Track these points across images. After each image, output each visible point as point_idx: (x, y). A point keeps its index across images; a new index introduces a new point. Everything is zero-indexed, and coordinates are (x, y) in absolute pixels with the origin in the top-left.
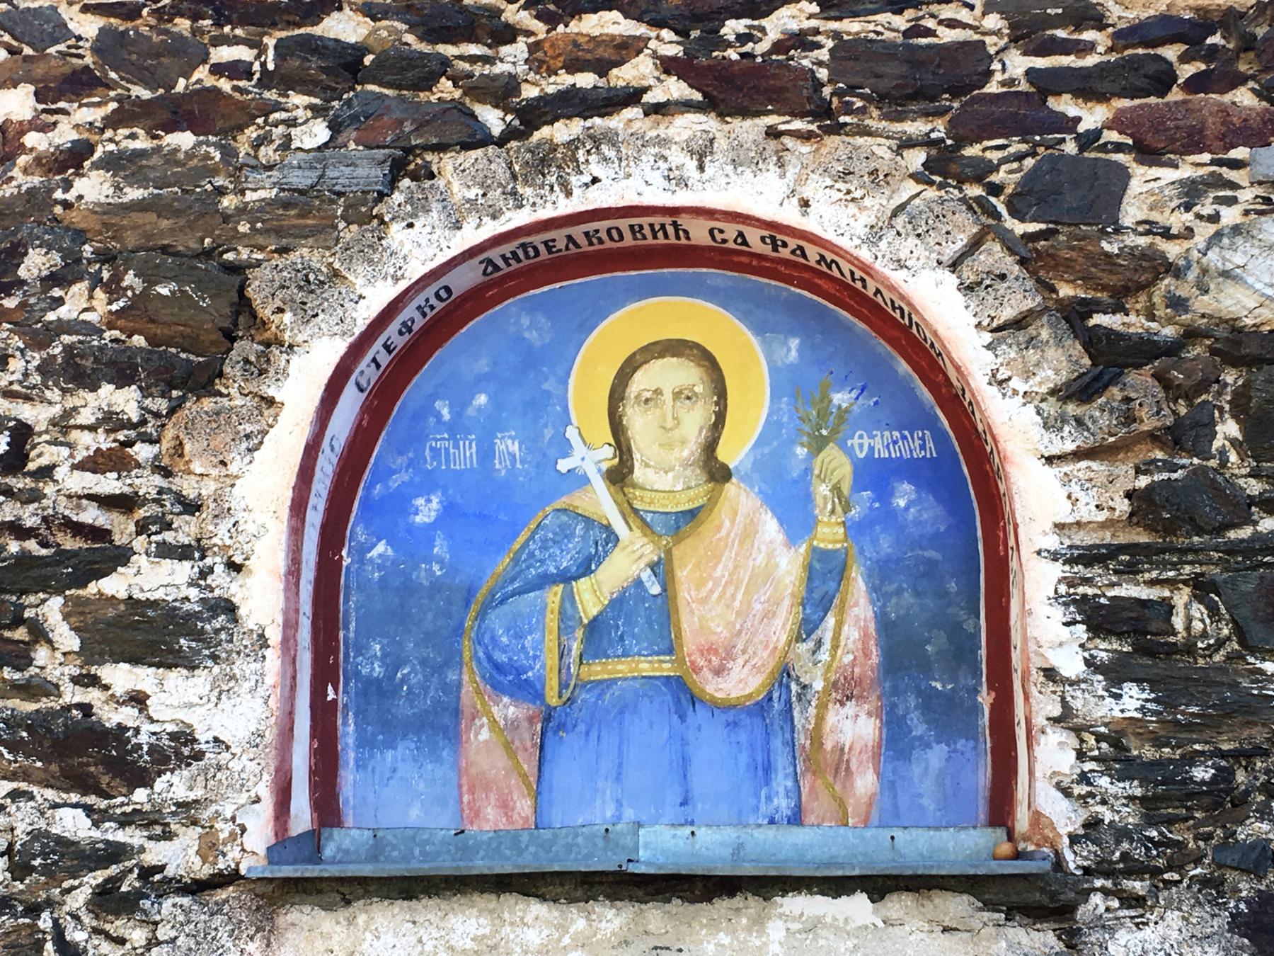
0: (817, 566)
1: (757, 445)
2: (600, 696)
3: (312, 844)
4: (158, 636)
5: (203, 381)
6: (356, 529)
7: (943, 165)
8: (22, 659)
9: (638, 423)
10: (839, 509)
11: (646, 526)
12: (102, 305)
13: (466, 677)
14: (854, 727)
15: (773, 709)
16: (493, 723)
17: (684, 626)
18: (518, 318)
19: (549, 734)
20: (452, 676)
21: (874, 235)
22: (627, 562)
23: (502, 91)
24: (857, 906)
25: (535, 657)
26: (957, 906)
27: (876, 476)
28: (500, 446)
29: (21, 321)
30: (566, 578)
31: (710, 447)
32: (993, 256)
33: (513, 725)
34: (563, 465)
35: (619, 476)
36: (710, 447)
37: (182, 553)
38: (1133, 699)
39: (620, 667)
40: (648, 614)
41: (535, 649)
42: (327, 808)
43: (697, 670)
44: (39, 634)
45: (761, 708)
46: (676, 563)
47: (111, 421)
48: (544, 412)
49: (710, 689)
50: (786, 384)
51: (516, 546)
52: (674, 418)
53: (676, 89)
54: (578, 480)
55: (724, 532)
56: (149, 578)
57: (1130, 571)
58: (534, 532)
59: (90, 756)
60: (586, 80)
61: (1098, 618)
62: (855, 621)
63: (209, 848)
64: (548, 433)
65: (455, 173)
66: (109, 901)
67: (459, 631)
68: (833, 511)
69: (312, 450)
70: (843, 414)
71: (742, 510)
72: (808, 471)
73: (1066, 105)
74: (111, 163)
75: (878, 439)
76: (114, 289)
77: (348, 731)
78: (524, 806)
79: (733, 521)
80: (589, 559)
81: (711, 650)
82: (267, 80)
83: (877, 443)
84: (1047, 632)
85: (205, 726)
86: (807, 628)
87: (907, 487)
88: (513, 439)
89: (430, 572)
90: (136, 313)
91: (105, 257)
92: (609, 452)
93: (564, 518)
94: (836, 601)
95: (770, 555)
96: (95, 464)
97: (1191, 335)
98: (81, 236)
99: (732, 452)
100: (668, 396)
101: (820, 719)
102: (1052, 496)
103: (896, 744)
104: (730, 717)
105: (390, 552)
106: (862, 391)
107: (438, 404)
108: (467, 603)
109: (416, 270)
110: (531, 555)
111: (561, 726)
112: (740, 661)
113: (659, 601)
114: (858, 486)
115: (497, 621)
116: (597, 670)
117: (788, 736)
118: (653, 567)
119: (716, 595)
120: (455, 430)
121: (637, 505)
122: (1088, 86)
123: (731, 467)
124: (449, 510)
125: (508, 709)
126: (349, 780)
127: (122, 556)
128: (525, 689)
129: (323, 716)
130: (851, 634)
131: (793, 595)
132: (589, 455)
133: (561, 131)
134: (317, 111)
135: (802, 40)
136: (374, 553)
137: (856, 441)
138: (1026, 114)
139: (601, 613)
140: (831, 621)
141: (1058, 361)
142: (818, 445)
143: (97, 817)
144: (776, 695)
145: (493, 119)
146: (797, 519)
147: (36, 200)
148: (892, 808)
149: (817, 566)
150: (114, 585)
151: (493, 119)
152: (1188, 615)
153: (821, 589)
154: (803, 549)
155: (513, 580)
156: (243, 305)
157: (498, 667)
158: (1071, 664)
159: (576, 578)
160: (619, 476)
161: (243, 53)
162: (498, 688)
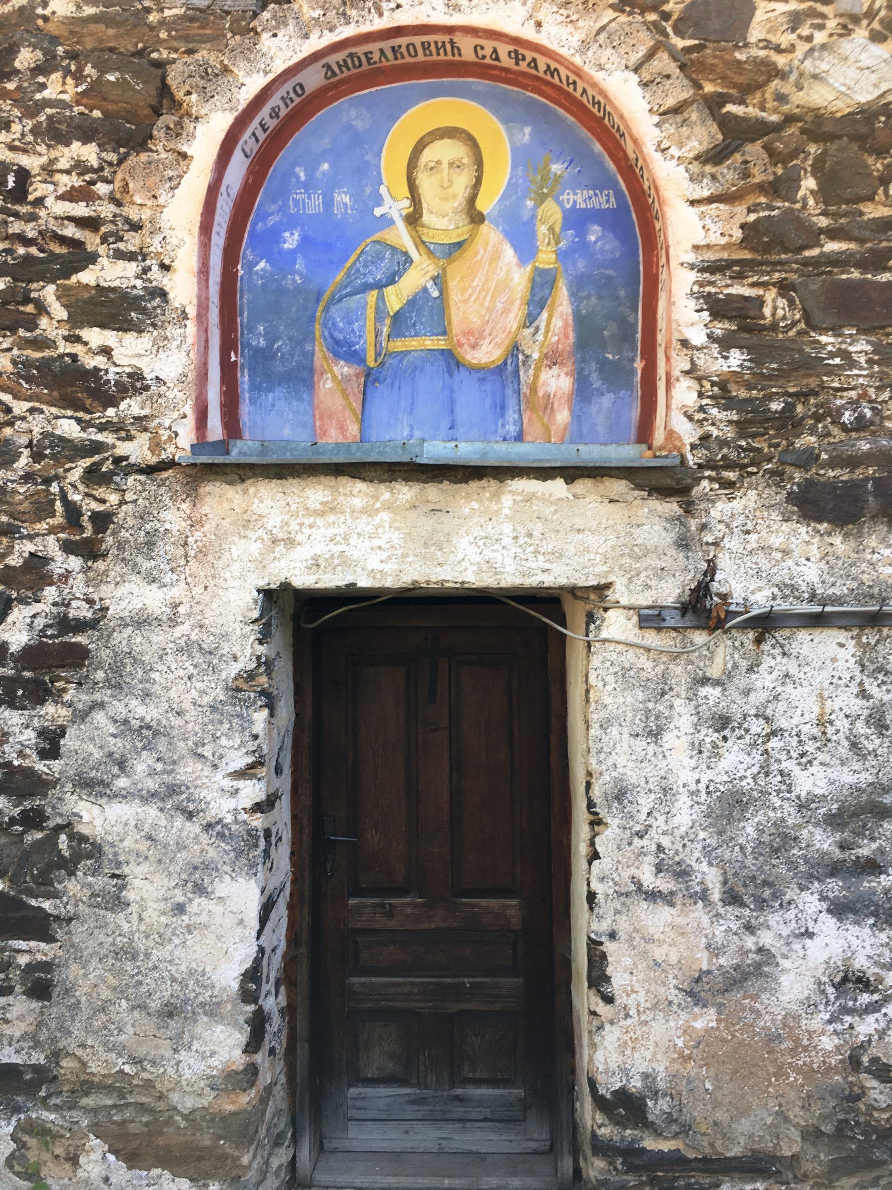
0: (538, 279)
1: (503, 198)
2: (400, 362)
3: (223, 447)
4: (117, 310)
5: (140, 141)
6: (246, 250)
8: (31, 325)
9: (426, 184)
10: (553, 242)
11: (430, 253)
12: (72, 90)
13: (317, 348)
14: (557, 382)
15: (508, 371)
16: (334, 379)
17: (453, 318)
18: (348, 112)
19: (369, 384)
20: (308, 348)
21: (585, 46)
22: (417, 277)
24: (558, 486)
25: (360, 336)
26: (618, 487)
27: (577, 220)
28: (337, 198)
29: (20, 99)
30: (380, 286)
31: (472, 200)
32: (663, 62)
33: (346, 379)
34: (378, 212)
35: (413, 219)
36: (472, 200)
37: (131, 257)
38: (736, 359)
39: (413, 343)
40: (429, 310)
41: (360, 331)
43: (461, 345)
44: (42, 309)
45: (500, 369)
46: (449, 277)
47: (80, 167)
48: (365, 175)
49: (468, 357)
50: (520, 157)
51: (348, 264)
52: (449, 181)
54: (387, 221)
55: (479, 257)
56: (109, 273)
57: (739, 277)
58: (359, 257)
59: (77, 387)
61: (718, 308)
63: (156, 445)
64: (368, 190)
66: (93, 476)
67: (312, 319)
68: (549, 244)
69: (213, 191)
70: (557, 178)
71: (491, 243)
72: (533, 217)
75: (579, 196)
76: (79, 77)
77: (244, 380)
78: (353, 429)
79: (485, 250)
80: (395, 274)
81: (469, 333)
83: (579, 198)
84: (684, 315)
85: (151, 368)
86: (530, 319)
87: (596, 228)
88: (346, 193)
89: (294, 280)
90: (95, 93)
91: (73, 56)
92: (407, 203)
93: (378, 247)
94: (549, 302)
95: (508, 272)
96: (70, 196)
97: (789, 119)
98: (55, 40)
99: (486, 204)
100: (445, 165)
101: (536, 377)
102: (692, 228)
103: (582, 392)
104: (481, 374)
105: (268, 267)
106: (571, 162)
107: (297, 169)
108: (318, 301)
109: (279, 66)
110: (358, 271)
111: (377, 380)
112: (488, 340)
113: (438, 301)
114: (566, 226)
115: (336, 313)
116: (399, 345)
117: (516, 387)
118: (435, 279)
119: (473, 299)
120: (308, 186)
121: (425, 239)
123: (485, 213)
124: (305, 240)
125: (343, 369)
126: (245, 410)
127: (93, 258)
128: (354, 356)
129: (229, 372)
130: (557, 323)
131: (521, 298)
132: (395, 206)
136: (258, 268)
137: (565, 197)
139: (401, 308)
140: (545, 315)
141: (702, 135)
142: (541, 199)
143: (85, 425)
144: (509, 361)
148: (578, 431)
149: (538, 279)
150: (87, 277)
152: (774, 306)
154: (529, 268)
155: (345, 288)
156: (165, 90)
157: (337, 342)
158: (698, 337)
159: (386, 286)
160: (413, 219)
162: (337, 355)
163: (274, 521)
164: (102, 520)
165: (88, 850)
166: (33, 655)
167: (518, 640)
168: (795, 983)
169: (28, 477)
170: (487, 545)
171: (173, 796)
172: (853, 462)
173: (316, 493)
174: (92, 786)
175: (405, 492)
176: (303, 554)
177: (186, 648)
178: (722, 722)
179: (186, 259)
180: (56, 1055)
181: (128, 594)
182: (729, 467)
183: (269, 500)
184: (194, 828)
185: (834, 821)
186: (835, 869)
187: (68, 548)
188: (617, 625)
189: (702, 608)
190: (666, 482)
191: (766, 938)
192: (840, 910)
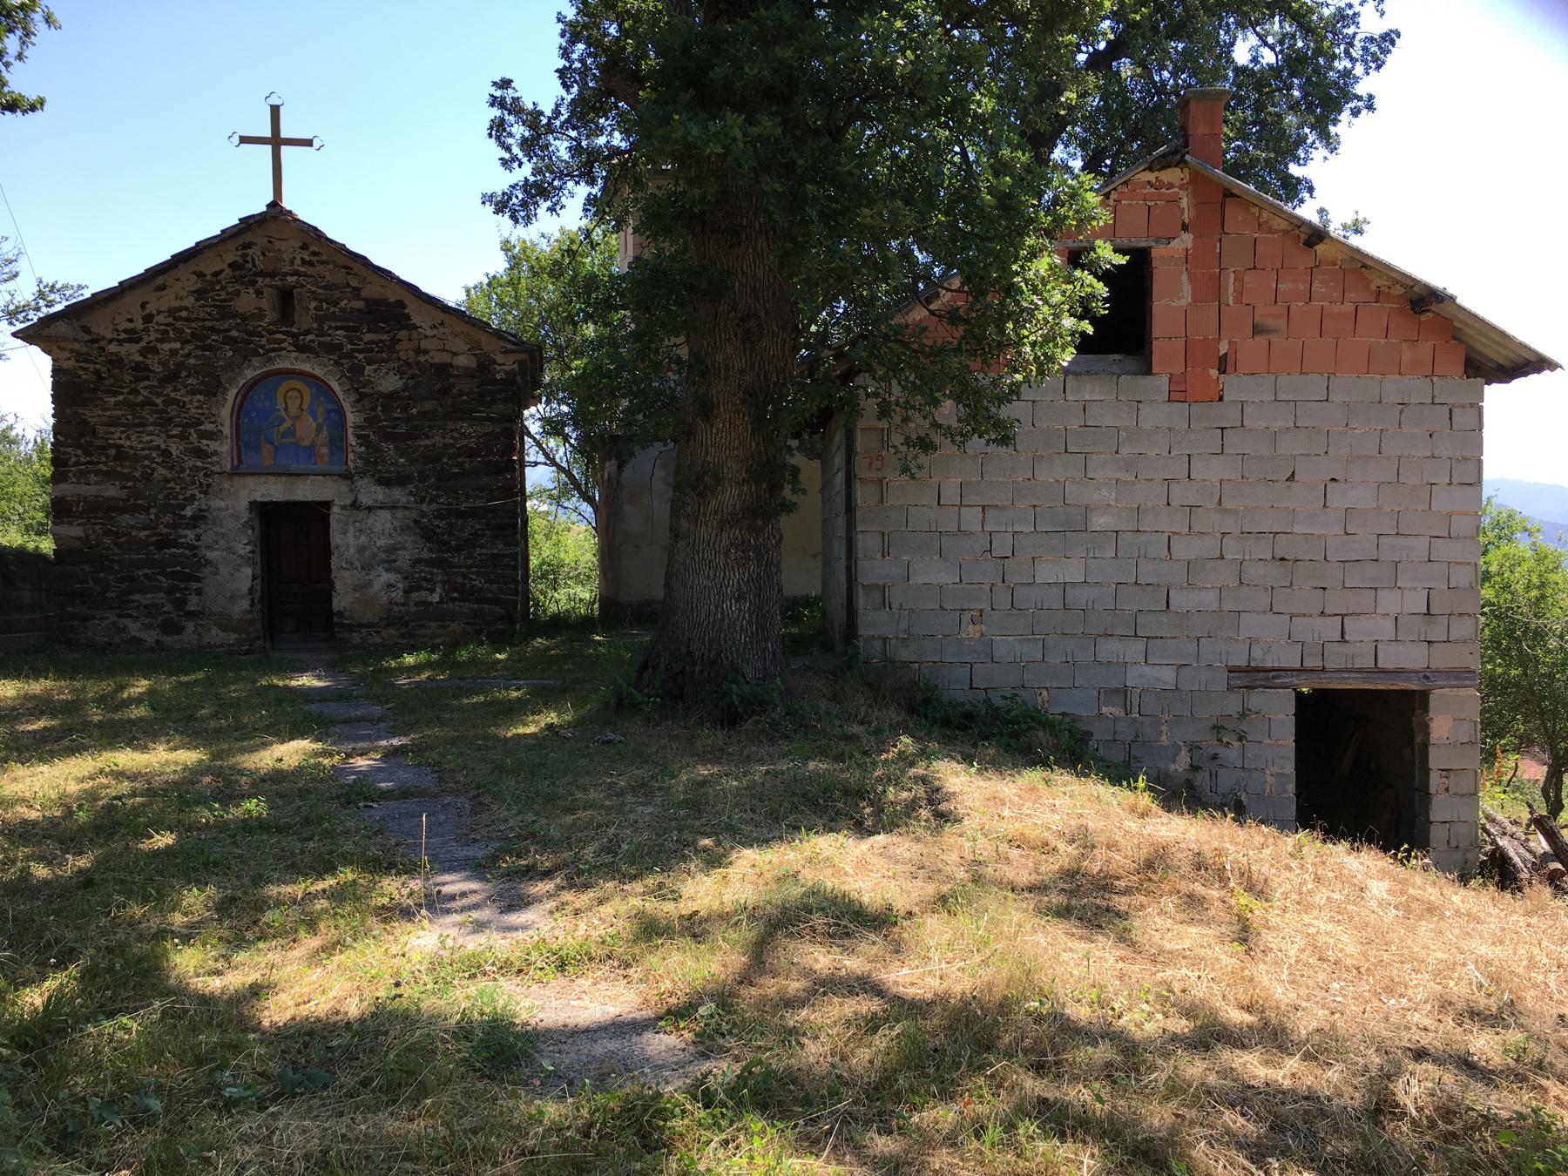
3: (238, 467)
4: (211, 436)
5: (214, 395)
14: (325, 450)
15: (311, 448)
16: (266, 449)
23: (263, 347)
27: (328, 411)
35: (286, 409)
40: (291, 432)
42: (240, 461)
56: (208, 427)
59: (200, 454)
61: (358, 436)
62: (325, 434)
65: (255, 361)
66: (205, 475)
83: (329, 406)
84: (352, 440)
90: (201, 383)
102: (351, 418)
103: (331, 453)
122: (359, 351)
128: (270, 442)
129: (238, 447)
132: (281, 406)
138: (350, 355)
146: (315, 418)
147: (183, 363)
153: (319, 429)
164: (209, 486)
165: (209, 562)
166: (191, 518)
167: (317, 513)
168: (376, 587)
170: (305, 491)
173: (262, 479)
174: (208, 547)
179: (227, 423)
181: (216, 503)
182: (362, 473)
183: (251, 482)
188: (335, 509)
189: (355, 505)
190: (347, 476)
192: (386, 570)
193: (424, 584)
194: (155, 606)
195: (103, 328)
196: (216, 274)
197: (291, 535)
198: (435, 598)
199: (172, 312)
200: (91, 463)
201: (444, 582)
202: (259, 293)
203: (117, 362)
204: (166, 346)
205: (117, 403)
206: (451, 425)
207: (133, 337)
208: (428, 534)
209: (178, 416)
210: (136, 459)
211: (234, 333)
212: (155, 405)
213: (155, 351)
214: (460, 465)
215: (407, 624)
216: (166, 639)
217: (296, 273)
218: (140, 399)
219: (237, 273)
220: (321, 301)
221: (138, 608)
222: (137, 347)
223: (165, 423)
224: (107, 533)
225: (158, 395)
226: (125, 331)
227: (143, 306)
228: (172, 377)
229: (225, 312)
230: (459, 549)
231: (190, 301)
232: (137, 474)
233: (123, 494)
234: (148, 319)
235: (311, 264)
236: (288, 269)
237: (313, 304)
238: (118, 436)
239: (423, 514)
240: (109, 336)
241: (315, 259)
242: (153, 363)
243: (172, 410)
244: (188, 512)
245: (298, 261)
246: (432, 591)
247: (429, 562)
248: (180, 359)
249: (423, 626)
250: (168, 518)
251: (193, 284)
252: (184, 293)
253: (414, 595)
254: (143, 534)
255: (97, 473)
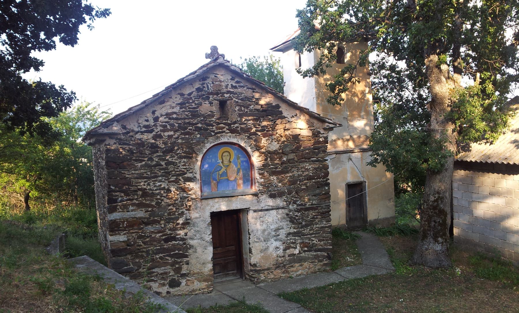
4: (190, 180)
5: (191, 158)
7: (249, 138)
9: (224, 158)
18: (214, 150)
22: (223, 169)
23: (213, 131)
35: (222, 162)
38: (262, 180)
47: (184, 162)
48: (216, 157)
53: (228, 131)
54: (219, 163)
56: (189, 175)
60: (221, 130)
61: (260, 174)
62: (241, 174)
63: (196, 196)
65: (210, 139)
73: (258, 133)
74: (181, 138)
82: (194, 130)
83: (242, 159)
86: (237, 174)
96: (183, 165)
109: (208, 148)
116: (221, 178)
120: (209, 159)
122: (259, 131)
125: (215, 182)
127: (186, 173)
128: (216, 180)
132: (220, 161)
133: (219, 135)
134: (198, 134)
135: (237, 127)
145: (213, 134)
146: (236, 166)
147: (175, 142)
150: (186, 176)
151: (213, 134)
158: (258, 178)
160: (222, 162)
161: (191, 128)
163: (211, 204)
164: (190, 206)
165: (192, 247)
166: (183, 224)
168: (271, 249)
169: (180, 202)
170: (236, 205)
171: (202, 238)
172: (275, 191)
173: (217, 200)
174: (192, 239)
175: (227, 199)
176: (215, 208)
177: (202, 221)
178: (263, 222)
180: (190, 271)
182: (262, 193)
183: (211, 202)
184: (204, 242)
185: (275, 231)
186: (275, 236)
187: (186, 210)
191: (268, 245)
192: (276, 240)
193: (292, 245)
194: (166, 273)
195: (133, 126)
196: (190, 94)
197: (229, 228)
198: (297, 251)
199: (168, 115)
200: (129, 200)
201: (301, 243)
202: (211, 103)
203: (141, 144)
204: (166, 134)
205: (142, 166)
206: (302, 165)
207: (149, 129)
208: (292, 220)
209: (174, 170)
210: (153, 195)
211: (200, 125)
212: (162, 166)
213: (160, 137)
214: (305, 184)
215: (284, 266)
216: (171, 290)
217: (228, 92)
218: (154, 163)
219: (200, 93)
220: (241, 106)
221: (156, 275)
222: (151, 135)
223: (167, 174)
224: (140, 237)
225: (164, 160)
226: (145, 126)
227: (154, 112)
228: (170, 150)
229: (195, 114)
230: (306, 226)
231: (177, 109)
232: (154, 203)
233: (147, 215)
234: (156, 119)
235: (235, 87)
236: (225, 90)
237: (237, 108)
238: (142, 184)
239: (290, 211)
240: (136, 129)
241: (237, 85)
242: (160, 143)
243: (171, 168)
244: (181, 221)
245: (230, 86)
246: (296, 248)
247: (294, 234)
248: (173, 140)
249: (292, 266)
250: (171, 225)
251: (178, 100)
252: (174, 105)
253: (288, 251)
254: (158, 235)
255: (133, 205)
